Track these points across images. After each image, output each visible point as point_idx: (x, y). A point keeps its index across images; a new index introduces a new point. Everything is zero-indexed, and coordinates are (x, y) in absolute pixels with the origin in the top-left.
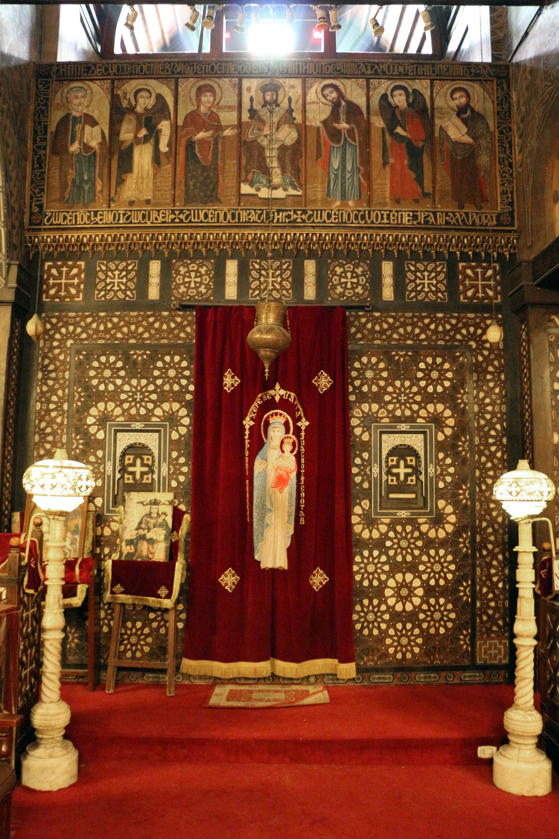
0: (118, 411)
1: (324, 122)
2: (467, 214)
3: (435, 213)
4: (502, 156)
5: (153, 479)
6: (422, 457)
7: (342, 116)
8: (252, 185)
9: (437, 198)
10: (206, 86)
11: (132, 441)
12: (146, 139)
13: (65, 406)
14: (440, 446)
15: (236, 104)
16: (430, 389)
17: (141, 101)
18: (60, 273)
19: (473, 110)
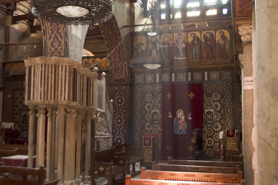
0: (151, 105)
1: (191, 42)
2: (223, 61)
3: (216, 61)
4: (231, 46)
5: (159, 119)
6: (214, 114)
7: (195, 40)
8: (177, 57)
9: (216, 58)
10: (166, 35)
11: (154, 111)
12: (154, 48)
13: (141, 105)
14: (217, 111)
15: (172, 39)
16: (215, 99)
17: (153, 39)
18: (138, 77)
19: (225, 36)
